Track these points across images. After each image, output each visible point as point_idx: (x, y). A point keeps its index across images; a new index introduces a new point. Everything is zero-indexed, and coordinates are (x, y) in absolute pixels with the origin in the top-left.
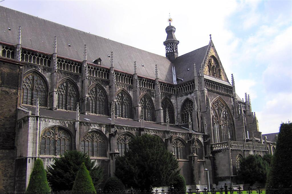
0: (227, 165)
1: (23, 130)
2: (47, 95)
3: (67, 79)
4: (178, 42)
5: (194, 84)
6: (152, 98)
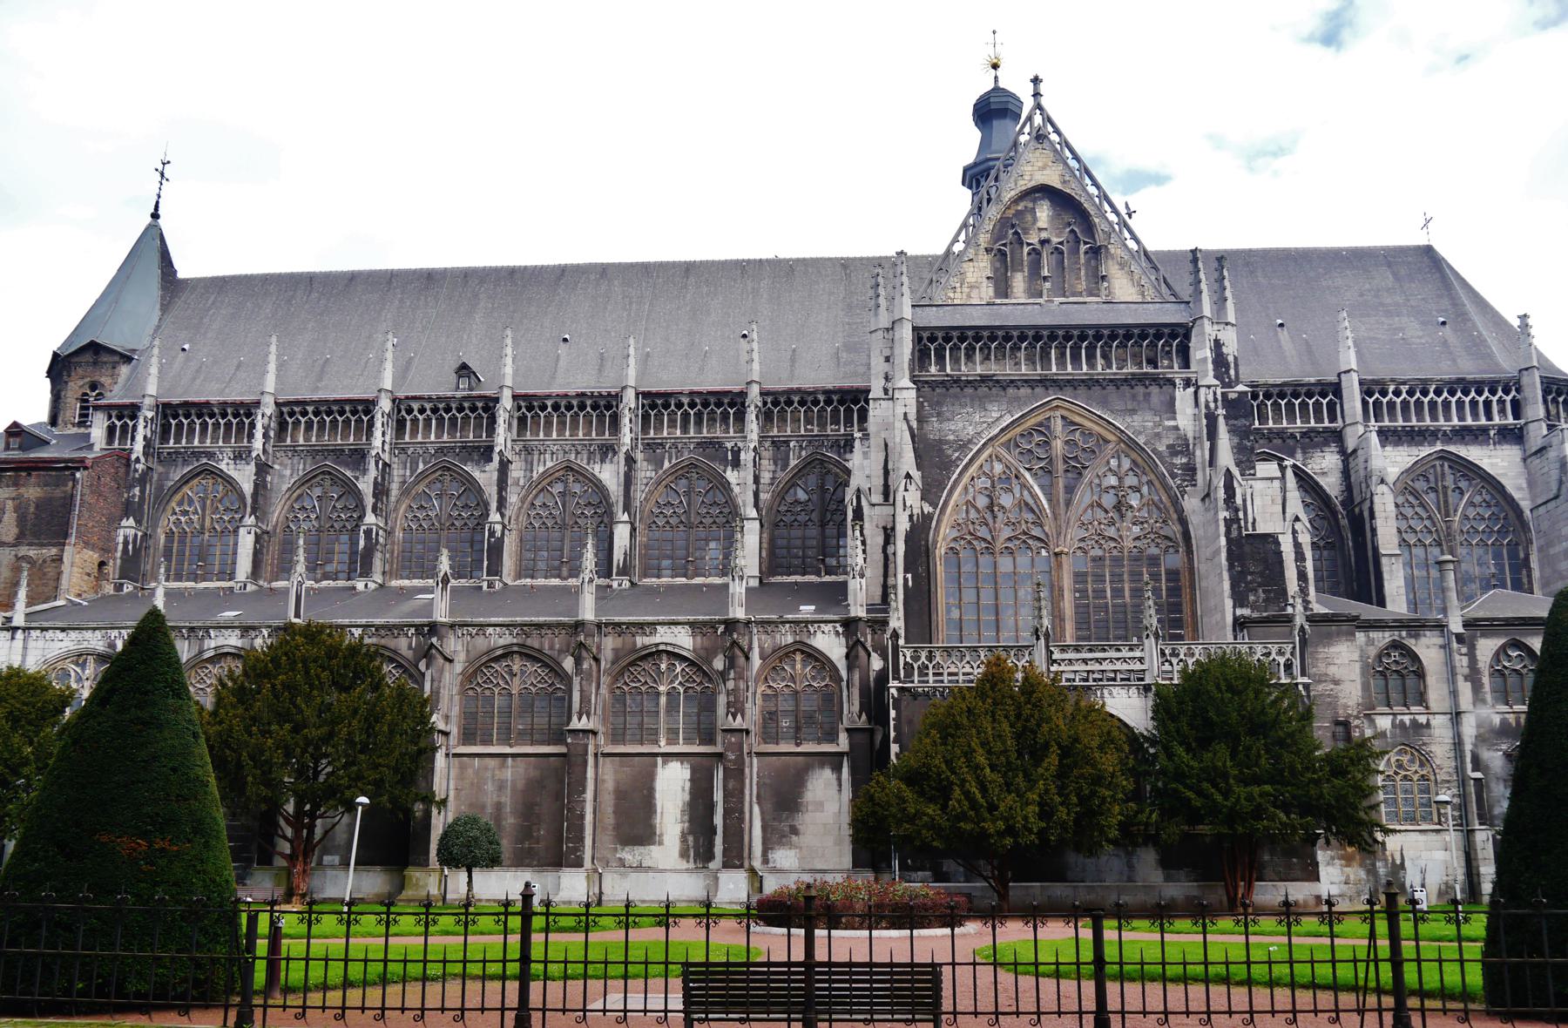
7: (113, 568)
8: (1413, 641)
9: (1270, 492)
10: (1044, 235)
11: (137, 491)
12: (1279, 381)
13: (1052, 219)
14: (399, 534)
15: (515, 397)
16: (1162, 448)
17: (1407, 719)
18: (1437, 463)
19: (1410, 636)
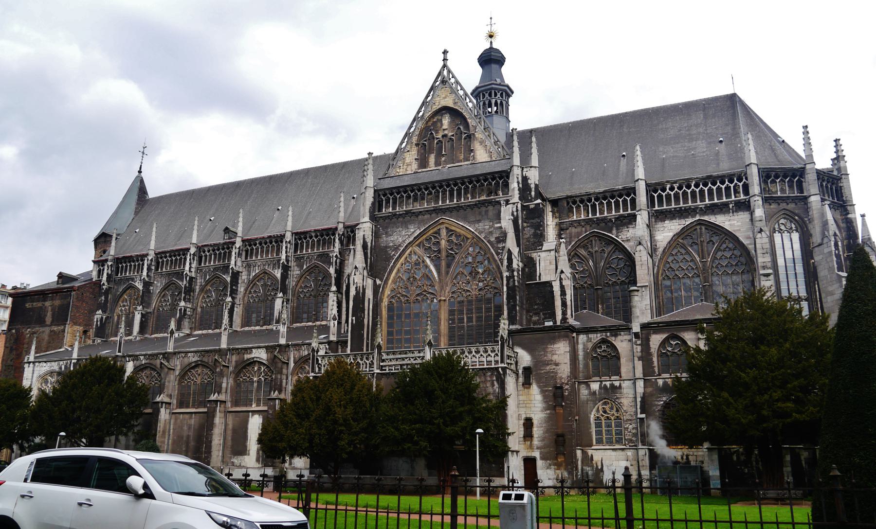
7: (92, 333)
8: (613, 338)
9: (549, 258)
10: (446, 132)
11: (103, 298)
12: (602, 190)
13: (450, 123)
14: (199, 310)
15: (243, 241)
16: (493, 239)
17: (608, 384)
18: (698, 227)
19: (612, 335)
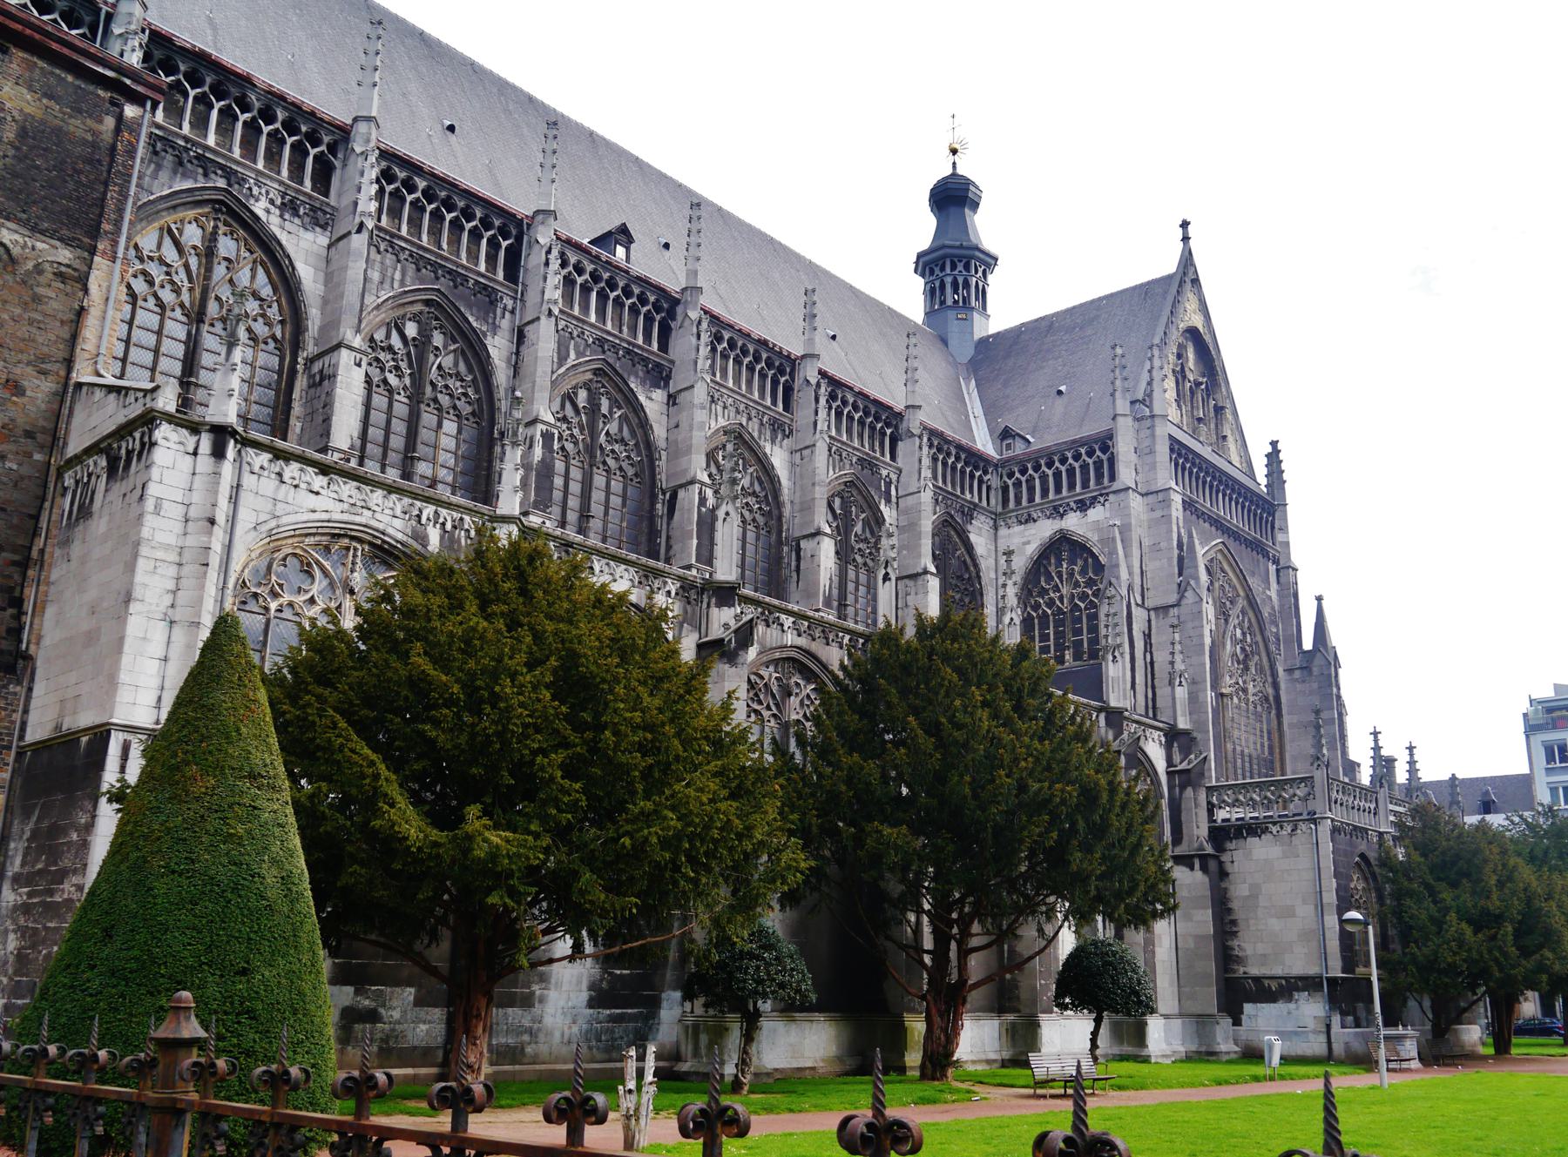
0: (1306, 911)
1: (99, 525)
2: (293, 372)
3: (427, 303)
4: (989, 261)
5: (1112, 461)
6: (882, 507)
13: (1196, 363)
